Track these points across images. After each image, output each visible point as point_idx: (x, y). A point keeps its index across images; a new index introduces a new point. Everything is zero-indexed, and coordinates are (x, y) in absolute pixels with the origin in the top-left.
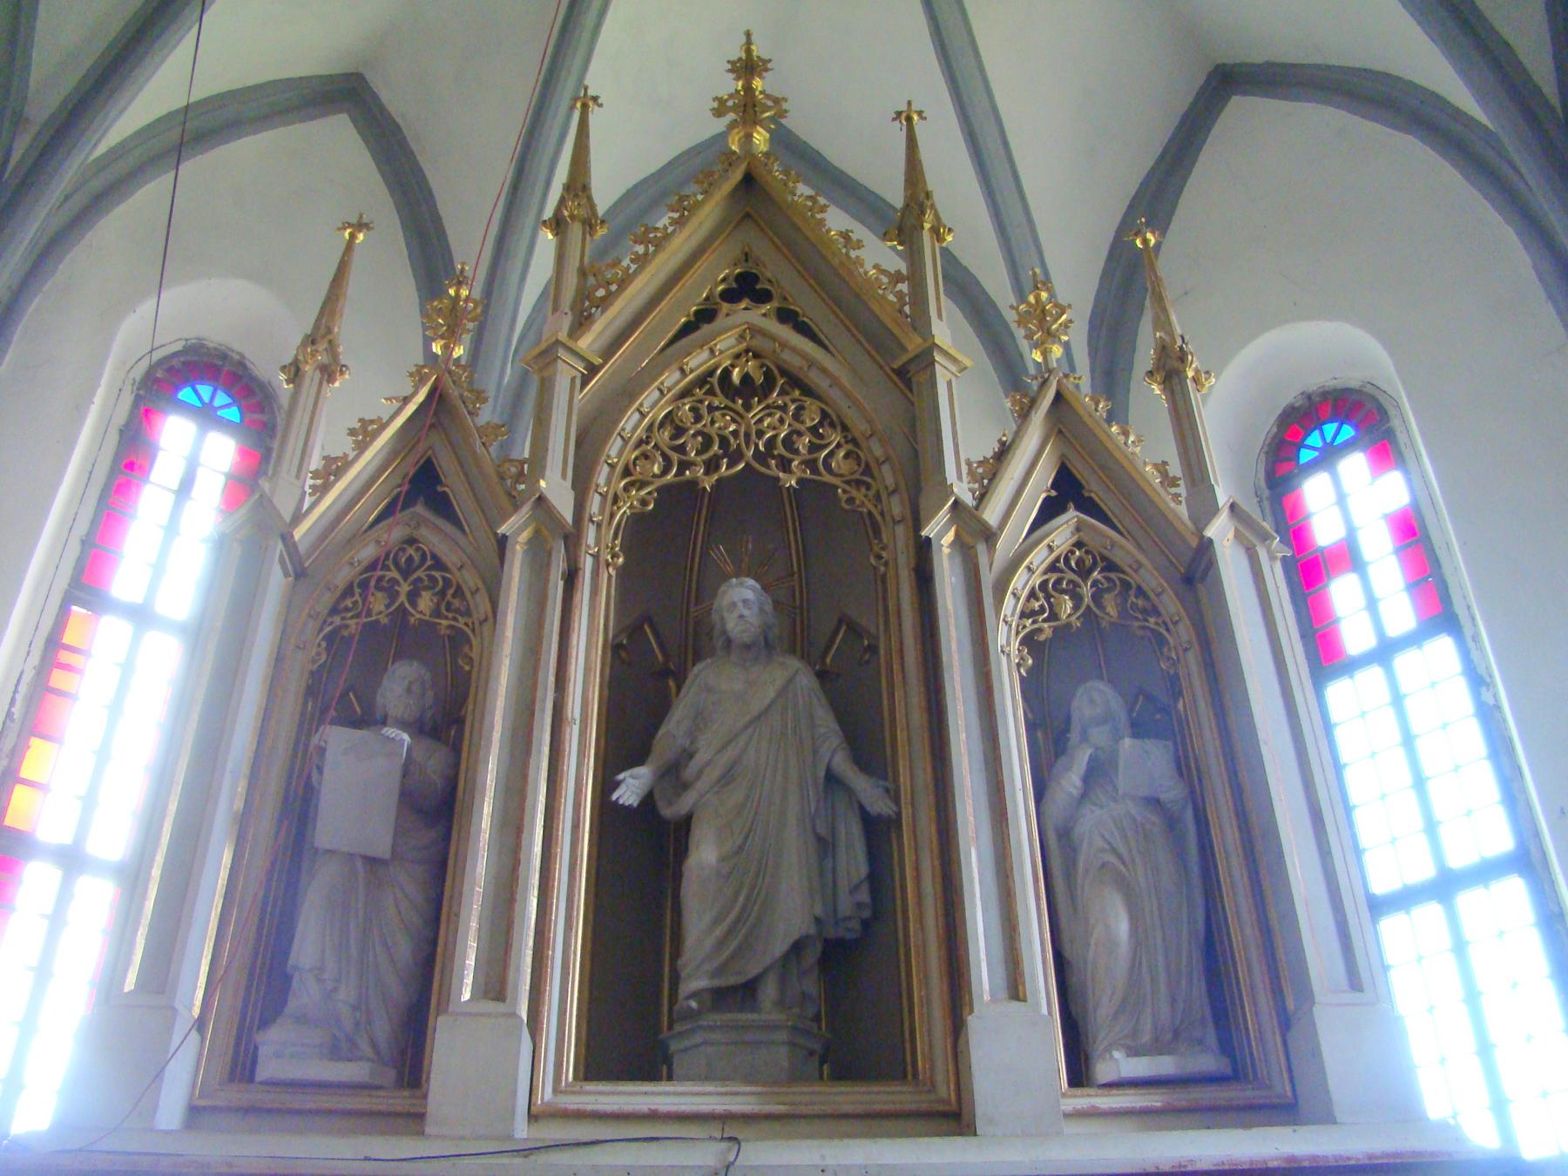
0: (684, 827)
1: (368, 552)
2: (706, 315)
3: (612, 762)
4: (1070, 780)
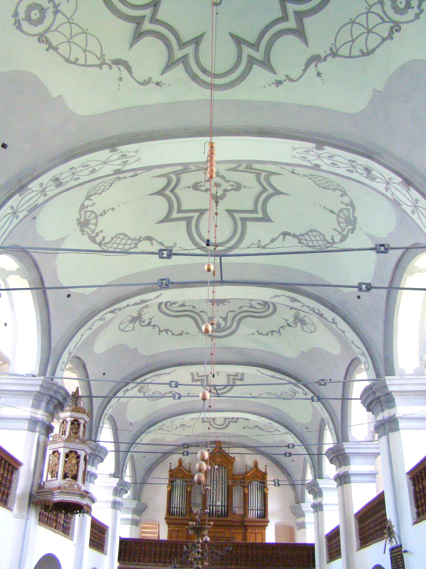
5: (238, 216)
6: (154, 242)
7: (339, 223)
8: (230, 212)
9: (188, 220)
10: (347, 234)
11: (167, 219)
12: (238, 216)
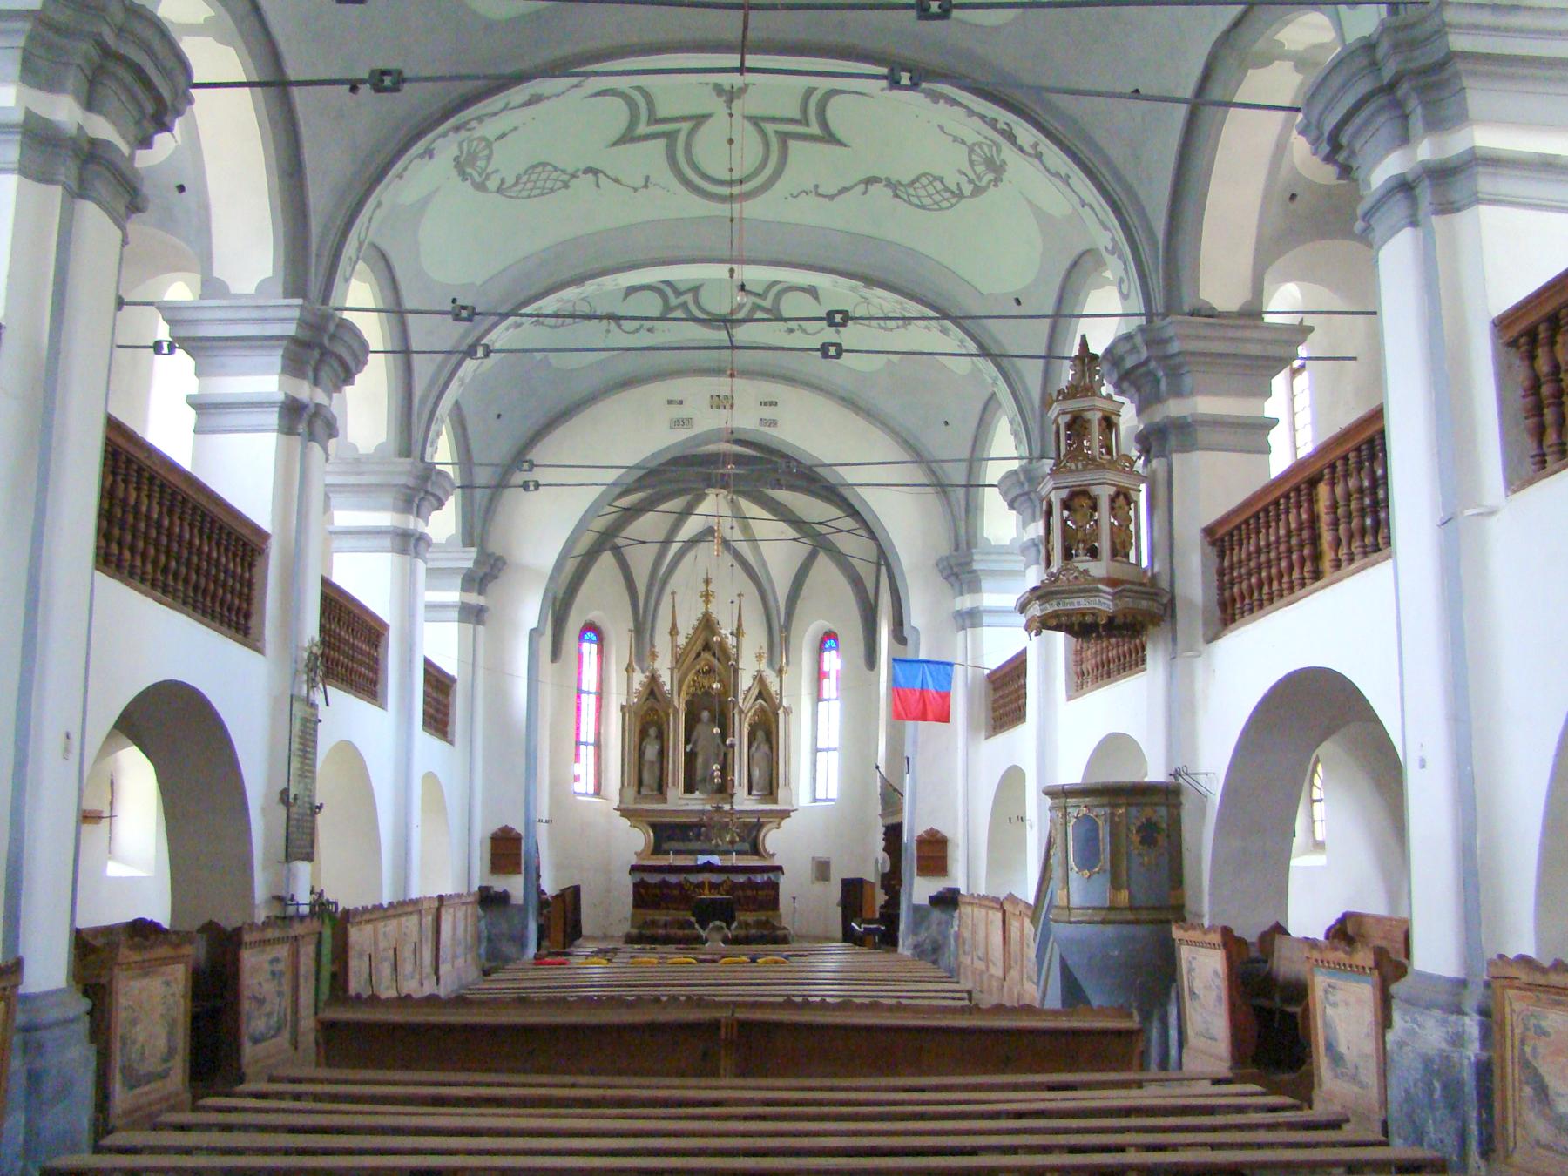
1: (645, 708)
2: (698, 655)
3: (687, 741)
4: (753, 749)
5: (770, 128)
6: (600, 175)
7: (972, 163)
8: (755, 121)
9: (671, 136)
10: (987, 187)
12: (770, 128)
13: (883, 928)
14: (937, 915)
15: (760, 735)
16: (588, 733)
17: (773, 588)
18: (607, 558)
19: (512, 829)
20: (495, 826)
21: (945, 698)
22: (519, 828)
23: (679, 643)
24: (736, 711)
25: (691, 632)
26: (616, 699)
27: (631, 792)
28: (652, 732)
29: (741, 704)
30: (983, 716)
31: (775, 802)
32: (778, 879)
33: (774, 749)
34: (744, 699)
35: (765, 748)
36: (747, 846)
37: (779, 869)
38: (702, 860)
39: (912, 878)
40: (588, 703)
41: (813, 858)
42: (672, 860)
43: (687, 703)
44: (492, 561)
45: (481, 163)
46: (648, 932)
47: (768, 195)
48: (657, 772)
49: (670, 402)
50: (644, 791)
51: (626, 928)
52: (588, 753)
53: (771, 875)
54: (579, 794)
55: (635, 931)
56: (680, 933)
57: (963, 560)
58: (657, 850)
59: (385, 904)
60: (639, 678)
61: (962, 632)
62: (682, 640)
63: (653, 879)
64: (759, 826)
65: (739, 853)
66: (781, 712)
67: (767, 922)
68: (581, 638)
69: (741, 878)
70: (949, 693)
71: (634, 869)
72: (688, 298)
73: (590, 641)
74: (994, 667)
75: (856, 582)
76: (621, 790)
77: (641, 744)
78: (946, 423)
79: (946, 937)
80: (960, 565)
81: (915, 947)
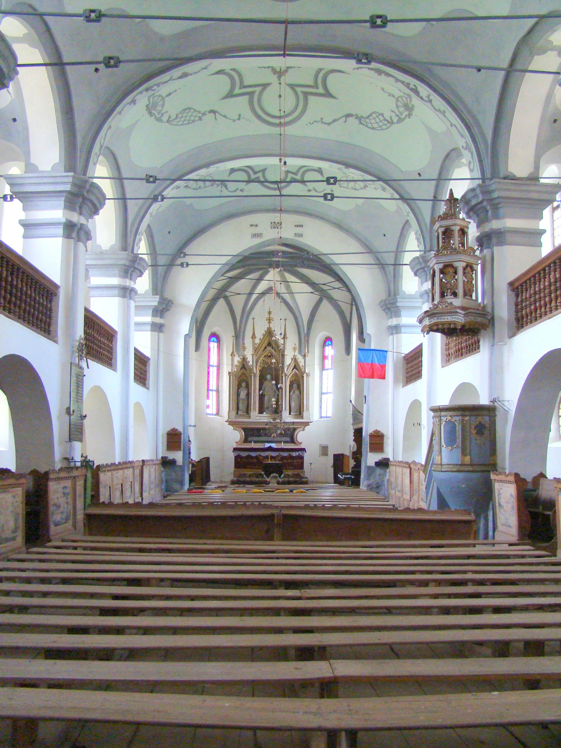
0: (264, 395)
1: (240, 374)
2: (266, 348)
3: (260, 390)
4: (292, 393)
5: (299, 90)
6: (217, 114)
7: (397, 106)
8: (292, 86)
11: (230, 95)
13: (353, 477)
14: (378, 471)
15: (295, 386)
16: (213, 386)
17: (301, 314)
18: (221, 302)
19: (177, 430)
20: (169, 429)
21: (383, 367)
22: (180, 429)
23: (256, 342)
24: (283, 375)
25: (262, 337)
26: (226, 369)
27: (234, 413)
28: (244, 384)
29: (286, 372)
30: (401, 377)
31: (302, 418)
32: (303, 454)
33: (302, 394)
34: (288, 369)
35: (297, 392)
36: (288, 439)
37: (304, 450)
38: (267, 445)
39: (367, 453)
40: (213, 371)
41: (320, 445)
42: (253, 445)
43: (260, 371)
44: (166, 302)
45: (159, 108)
46: (241, 479)
47: (299, 123)
48: (246, 404)
49: (251, 226)
50: (240, 413)
51: (231, 477)
52: (213, 395)
53: (300, 453)
54: (208, 414)
55: (235, 479)
56: (257, 480)
57: (392, 301)
58: (246, 441)
59: (117, 463)
60: (237, 359)
61: (391, 336)
62: (257, 341)
63: (244, 454)
64: (295, 429)
65: (285, 442)
66: (305, 375)
67: (298, 475)
68: (209, 340)
69: (286, 454)
70: (385, 366)
71: (235, 449)
72: (260, 175)
73: (213, 341)
74: (407, 353)
75: (341, 314)
76: (229, 413)
77: (238, 391)
78: (385, 235)
79: (383, 481)
80: (390, 304)
81: (368, 486)
